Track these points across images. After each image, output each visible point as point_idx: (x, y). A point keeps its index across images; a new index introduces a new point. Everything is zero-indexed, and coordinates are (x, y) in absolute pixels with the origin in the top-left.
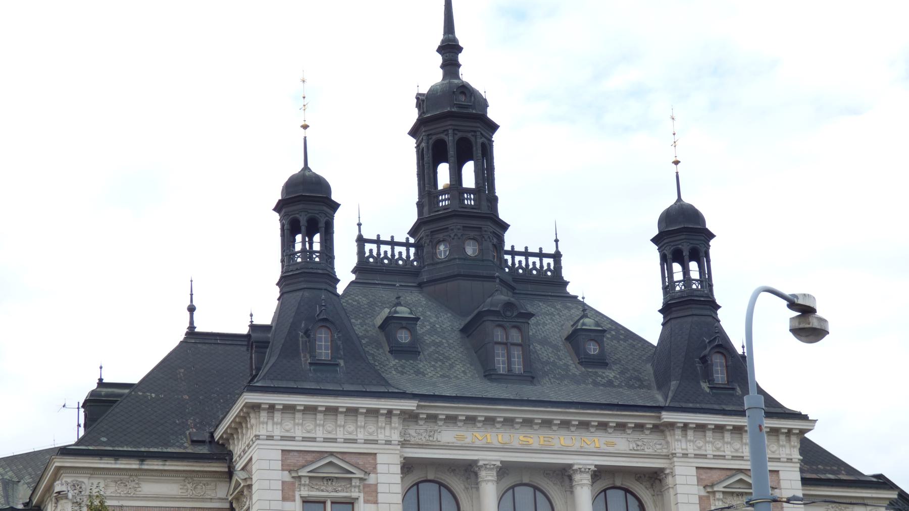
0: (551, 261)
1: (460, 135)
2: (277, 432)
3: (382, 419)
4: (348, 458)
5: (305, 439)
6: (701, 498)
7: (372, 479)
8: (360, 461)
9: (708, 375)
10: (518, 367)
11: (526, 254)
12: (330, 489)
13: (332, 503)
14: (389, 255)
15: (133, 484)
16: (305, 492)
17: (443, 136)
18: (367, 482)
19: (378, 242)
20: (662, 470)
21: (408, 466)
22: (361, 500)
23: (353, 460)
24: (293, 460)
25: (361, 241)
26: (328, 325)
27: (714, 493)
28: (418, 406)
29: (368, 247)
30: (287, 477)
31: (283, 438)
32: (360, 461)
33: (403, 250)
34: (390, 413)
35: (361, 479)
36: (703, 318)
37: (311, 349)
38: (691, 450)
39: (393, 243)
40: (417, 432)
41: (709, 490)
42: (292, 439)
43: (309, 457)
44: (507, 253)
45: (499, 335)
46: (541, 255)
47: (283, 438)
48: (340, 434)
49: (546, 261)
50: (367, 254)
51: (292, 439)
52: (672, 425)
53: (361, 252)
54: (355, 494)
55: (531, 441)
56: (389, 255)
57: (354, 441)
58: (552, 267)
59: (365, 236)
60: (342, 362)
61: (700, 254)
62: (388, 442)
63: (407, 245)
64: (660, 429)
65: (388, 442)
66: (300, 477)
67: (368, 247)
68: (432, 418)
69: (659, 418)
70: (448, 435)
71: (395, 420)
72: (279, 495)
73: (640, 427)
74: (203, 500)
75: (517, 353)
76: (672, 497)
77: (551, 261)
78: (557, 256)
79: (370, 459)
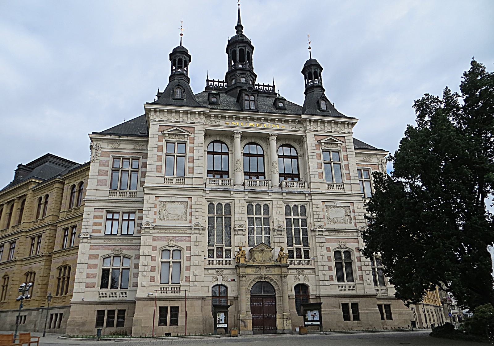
0: (272, 88)
1: (240, 48)
2: (157, 119)
3: (197, 116)
4: (184, 128)
5: (167, 121)
6: (316, 145)
7: (192, 136)
8: (188, 129)
9: (319, 107)
10: (253, 108)
11: (263, 86)
12: (176, 138)
13: (178, 143)
14: (217, 85)
15: (117, 145)
16: (167, 139)
17: (235, 49)
18: (190, 136)
19: (214, 81)
20: (302, 136)
21: (208, 134)
22: (188, 142)
23: (184, 128)
24: (162, 129)
25: (208, 81)
26: (180, 87)
27: (321, 143)
28: (210, 111)
29: (210, 83)
30: (160, 133)
31: (159, 121)
32: (188, 129)
33: (222, 84)
34: (199, 113)
35: (188, 135)
36: (319, 92)
37: (173, 95)
38: (312, 129)
39: (218, 82)
40: (212, 121)
41: (319, 142)
42: (163, 121)
43: (169, 127)
44: (256, 85)
45: (246, 98)
46: (268, 86)
47: (159, 121)
48: (181, 120)
49: (270, 88)
50: (210, 85)
51: (163, 121)
52: (305, 120)
53: (208, 84)
54: (186, 140)
55: (253, 125)
56: (217, 85)
57: (186, 123)
58: (272, 90)
59: (209, 79)
60: (185, 100)
61: (317, 75)
62: (199, 123)
63: (223, 82)
64: (302, 122)
65: (199, 123)
66: (165, 134)
67: (210, 83)
68: (216, 117)
69: (301, 118)
70: (222, 122)
71: (202, 116)
72: (157, 140)
73: (293, 121)
74: (142, 150)
75: (252, 103)
76: (306, 144)
77: (272, 88)
78: (274, 86)
79: (192, 129)
